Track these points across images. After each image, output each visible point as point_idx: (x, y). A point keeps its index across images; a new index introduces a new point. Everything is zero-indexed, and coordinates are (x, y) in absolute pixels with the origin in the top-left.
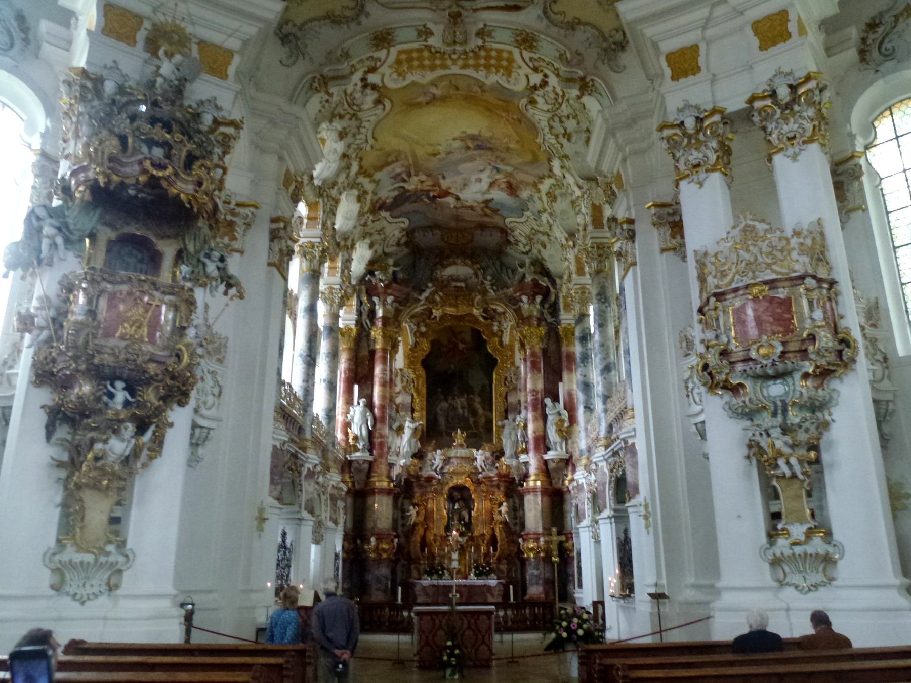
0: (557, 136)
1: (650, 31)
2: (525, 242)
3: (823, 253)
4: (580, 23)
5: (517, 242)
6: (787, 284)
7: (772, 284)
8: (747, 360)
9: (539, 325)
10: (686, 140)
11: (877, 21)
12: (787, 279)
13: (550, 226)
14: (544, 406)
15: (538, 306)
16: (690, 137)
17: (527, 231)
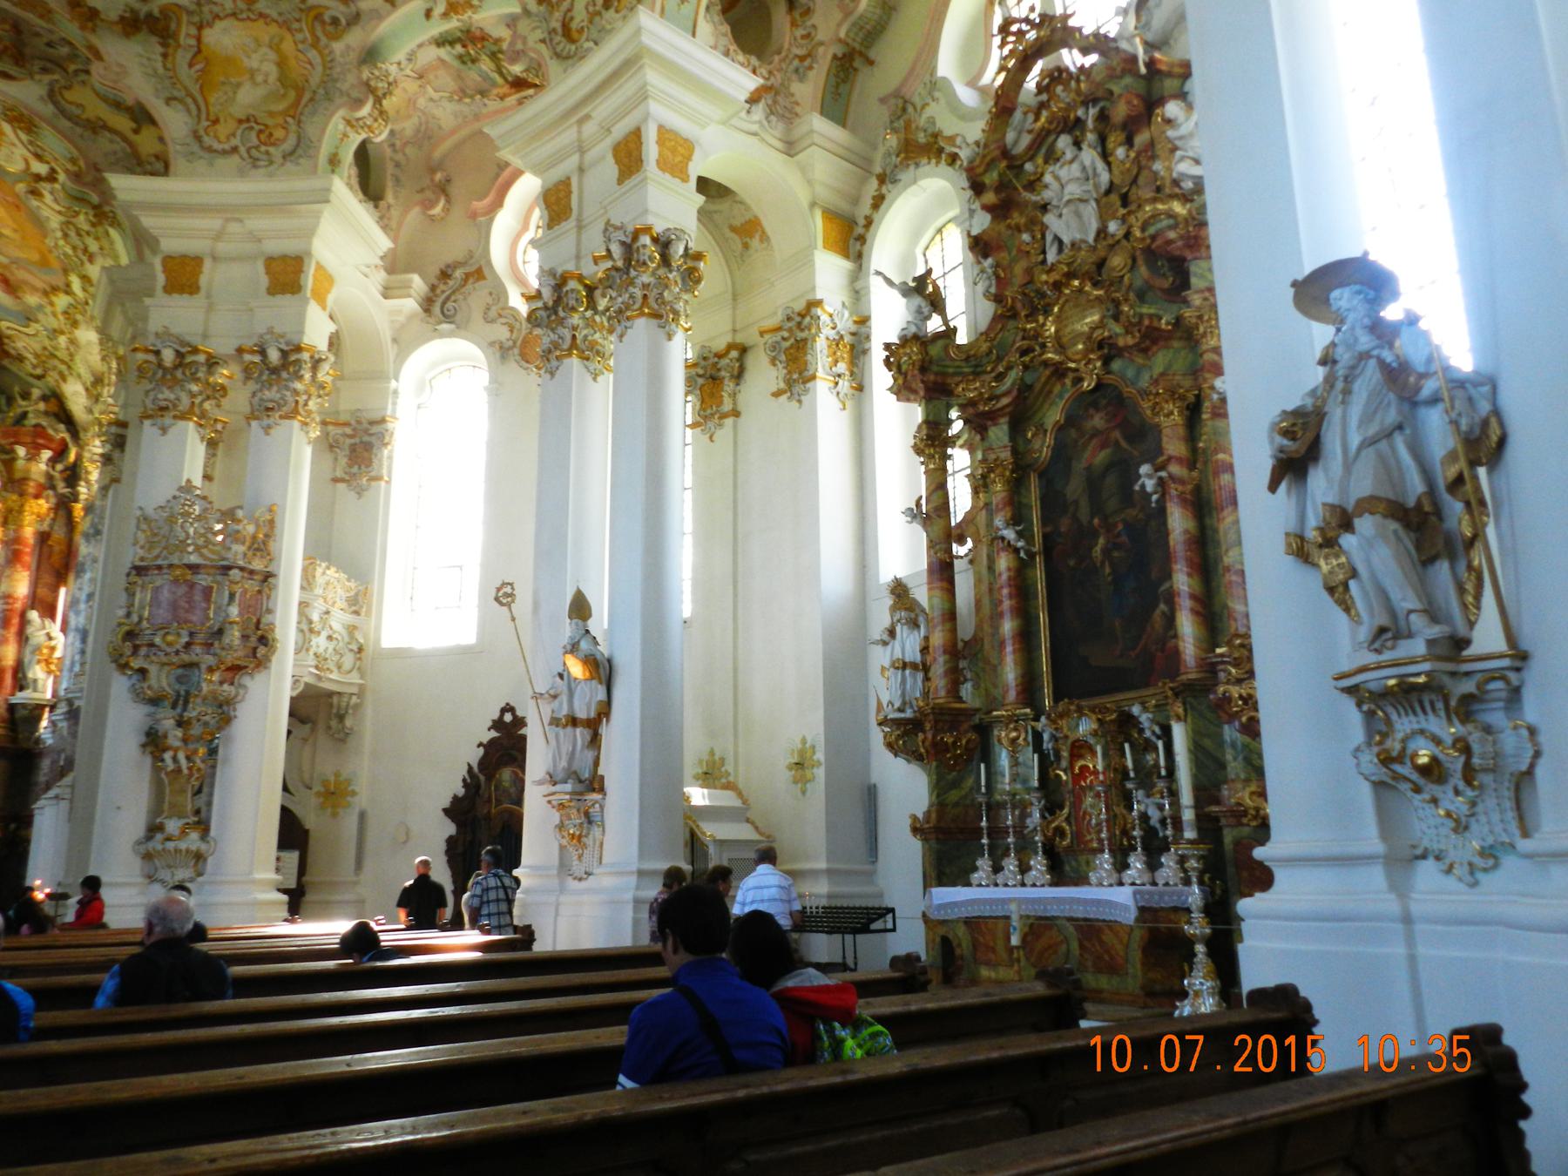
0: (74, 248)
1: (148, 221)
2: (35, 361)
3: (264, 543)
4: (105, 127)
5: (20, 359)
6: (212, 571)
7: (194, 568)
8: (152, 645)
9: (37, 497)
10: (160, 373)
11: (449, 272)
12: (212, 567)
13: (71, 355)
14: (24, 622)
15: (43, 467)
16: (165, 369)
17: (37, 347)
